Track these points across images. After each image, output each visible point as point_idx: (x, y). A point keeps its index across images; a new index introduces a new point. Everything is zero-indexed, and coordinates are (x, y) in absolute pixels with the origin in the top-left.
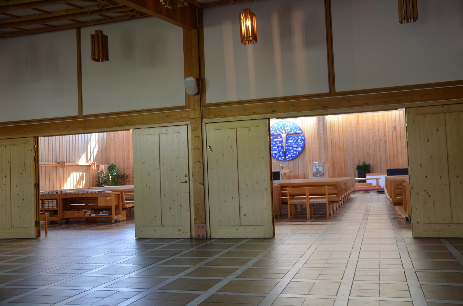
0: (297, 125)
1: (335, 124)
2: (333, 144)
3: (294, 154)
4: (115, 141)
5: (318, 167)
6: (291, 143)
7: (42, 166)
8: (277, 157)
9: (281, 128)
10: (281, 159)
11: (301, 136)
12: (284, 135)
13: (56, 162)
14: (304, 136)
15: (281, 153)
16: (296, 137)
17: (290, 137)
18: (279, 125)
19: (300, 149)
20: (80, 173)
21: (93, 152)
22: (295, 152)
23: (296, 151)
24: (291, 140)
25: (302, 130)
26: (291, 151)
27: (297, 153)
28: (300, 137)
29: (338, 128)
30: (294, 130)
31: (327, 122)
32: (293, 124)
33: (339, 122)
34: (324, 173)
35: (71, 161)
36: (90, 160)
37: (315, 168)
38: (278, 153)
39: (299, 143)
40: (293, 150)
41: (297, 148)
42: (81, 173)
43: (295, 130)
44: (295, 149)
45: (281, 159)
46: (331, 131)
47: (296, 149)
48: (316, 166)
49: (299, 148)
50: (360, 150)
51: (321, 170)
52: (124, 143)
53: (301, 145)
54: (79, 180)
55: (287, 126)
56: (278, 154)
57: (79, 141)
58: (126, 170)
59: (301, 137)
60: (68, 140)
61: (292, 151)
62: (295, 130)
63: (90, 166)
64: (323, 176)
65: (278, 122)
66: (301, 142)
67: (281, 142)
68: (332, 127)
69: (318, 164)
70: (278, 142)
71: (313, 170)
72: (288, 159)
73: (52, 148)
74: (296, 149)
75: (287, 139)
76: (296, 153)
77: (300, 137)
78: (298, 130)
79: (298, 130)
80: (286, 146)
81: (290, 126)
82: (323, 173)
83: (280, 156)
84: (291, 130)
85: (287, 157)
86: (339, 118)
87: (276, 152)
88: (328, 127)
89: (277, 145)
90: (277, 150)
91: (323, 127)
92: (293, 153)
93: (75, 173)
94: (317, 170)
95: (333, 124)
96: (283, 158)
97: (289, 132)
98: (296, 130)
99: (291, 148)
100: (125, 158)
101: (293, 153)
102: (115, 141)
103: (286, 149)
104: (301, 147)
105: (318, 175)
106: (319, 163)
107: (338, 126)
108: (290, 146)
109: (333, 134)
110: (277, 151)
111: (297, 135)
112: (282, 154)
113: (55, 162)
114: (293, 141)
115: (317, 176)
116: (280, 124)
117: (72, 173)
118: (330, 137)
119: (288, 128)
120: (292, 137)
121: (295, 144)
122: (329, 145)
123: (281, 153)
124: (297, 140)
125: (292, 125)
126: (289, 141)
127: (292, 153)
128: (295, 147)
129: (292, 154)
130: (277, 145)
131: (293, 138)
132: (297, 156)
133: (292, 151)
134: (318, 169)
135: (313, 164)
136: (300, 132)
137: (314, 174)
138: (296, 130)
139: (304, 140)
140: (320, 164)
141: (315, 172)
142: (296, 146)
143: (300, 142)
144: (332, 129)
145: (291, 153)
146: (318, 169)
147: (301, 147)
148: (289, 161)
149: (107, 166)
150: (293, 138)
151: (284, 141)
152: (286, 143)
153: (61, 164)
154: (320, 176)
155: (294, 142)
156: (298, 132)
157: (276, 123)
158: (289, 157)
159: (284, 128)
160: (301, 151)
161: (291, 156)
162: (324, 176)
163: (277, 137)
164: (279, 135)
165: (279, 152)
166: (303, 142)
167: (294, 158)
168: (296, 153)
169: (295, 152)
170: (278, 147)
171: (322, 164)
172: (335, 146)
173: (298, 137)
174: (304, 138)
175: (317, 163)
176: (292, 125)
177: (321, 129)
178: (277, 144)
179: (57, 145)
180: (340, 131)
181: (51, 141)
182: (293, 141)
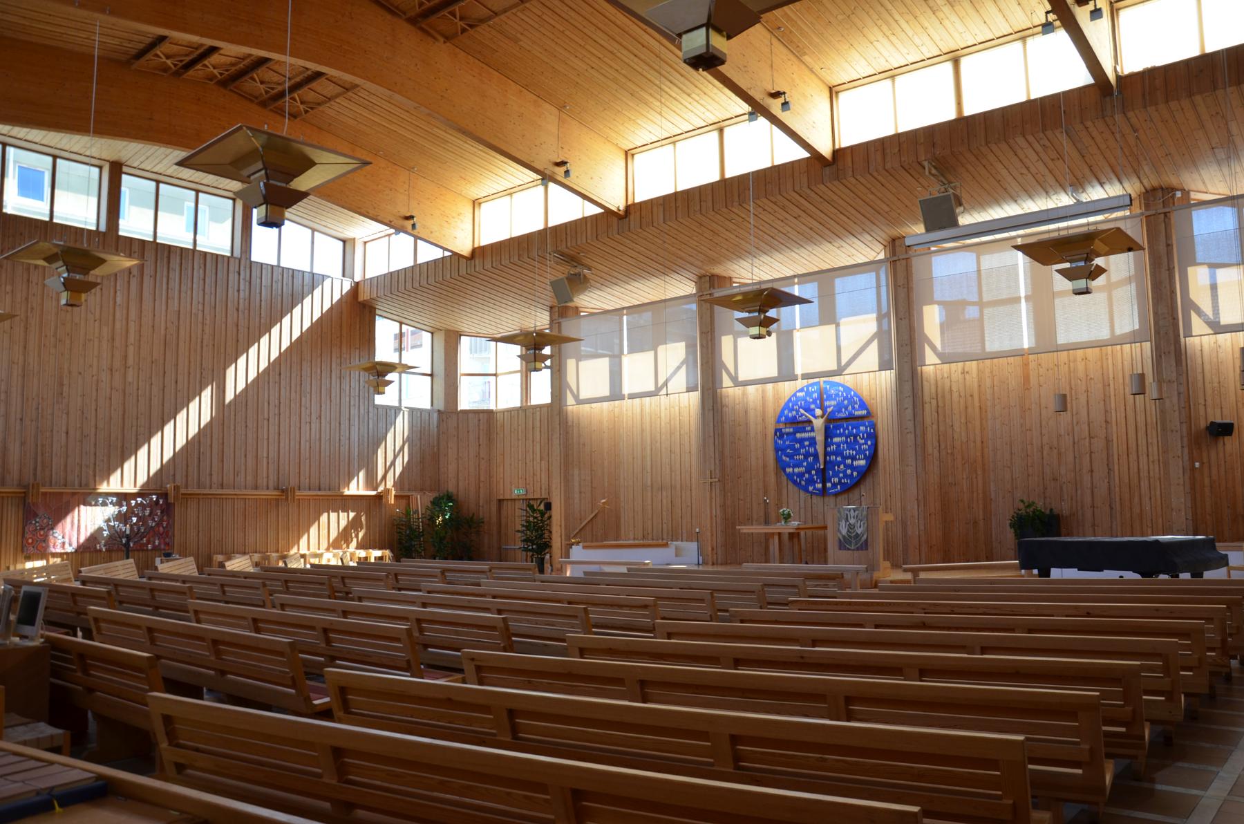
0: (856, 394)
1: (954, 389)
2: (946, 447)
3: (846, 476)
4: (458, 438)
5: (852, 521)
6: (838, 445)
7: (235, 497)
8: (803, 483)
9: (814, 402)
10: (815, 489)
11: (864, 425)
12: (819, 423)
13: (277, 488)
14: (874, 426)
15: (813, 472)
16: (852, 429)
17: (838, 428)
18: (809, 393)
19: (863, 462)
20: (341, 514)
21: (393, 463)
22: (849, 472)
23: (851, 467)
24: (840, 435)
25: (869, 407)
26: (839, 467)
27: (855, 474)
28: (862, 428)
29: (962, 401)
30: (846, 409)
31: (925, 383)
32: (844, 391)
33: (967, 383)
34: (869, 540)
35: (322, 486)
36: (383, 483)
37: (843, 523)
38: (806, 472)
39: (860, 445)
40: (846, 466)
41: (853, 458)
42: (352, 515)
43: (850, 408)
44: (849, 462)
45: (815, 489)
46: (940, 410)
47: (852, 462)
48: (847, 520)
49: (859, 459)
50: (766, 493)
51: (859, 531)
52: (479, 441)
53: (866, 450)
54: (345, 528)
55: (829, 397)
56: (807, 476)
57: (352, 440)
58: (483, 507)
59: (866, 427)
60: (318, 437)
61: (842, 466)
62: (850, 408)
63: (379, 497)
64: (867, 549)
65: (807, 386)
66: (866, 443)
67: (813, 442)
68: (943, 397)
69: (852, 511)
70: (807, 443)
71: (839, 531)
72: (830, 489)
73: (268, 457)
74: (852, 462)
75: (828, 434)
76: (852, 473)
77: (862, 428)
78: (856, 406)
79: (856, 406)
80: (826, 454)
81: (837, 395)
82: (866, 541)
83: (811, 481)
84: (839, 407)
85: (829, 485)
86: (966, 370)
87: (802, 470)
88: (927, 398)
89: (803, 451)
90: (805, 464)
91: (912, 398)
92: (845, 472)
93: (336, 514)
94: (848, 531)
95: (947, 389)
96: (819, 486)
97: (832, 412)
98: (853, 408)
99: (839, 459)
100: (482, 479)
101: (845, 472)
102: (458, 438)
103: (825, 462)
104: (865, 457)
105: (850, 545)
106: (854, 510)
107: (963, 394)
108: (837, 453)
109: (945, 417)
110: (803, 466)
111: (854, 422)
112: (816, 474)
113: (275, 489)
114: (844, 438)
115: (849, 549)
116: (813, 392)
117: (325, 515)
118: (935, 427)
119: (831, 404)
120: (843, 427)
121: (851, 448)
122: (930, 451)
123: (813, 472)
124: (855, 438)
125: (842, 394)
126: (836, 440)
127: (841, 472)
128: (848, 458)
129: (841, 475)
130: (803, 451)
131: (844, 430)
132: (855, 481)
133: (842, 466)
134: (851, 527)
135: (839, 512)
136: (864, 412)
137: (840, 540)
138: (853, 408)
139: (873, 437)
140: (857, 512)
141: (844, 537)
142: (853, 452)
143: (863, 441)
144: (940, 404)
145: (839, 472)
146: (851, 527)
147: (865, 455)
148: (836, 495)
149: (431, 496)
150: (844, 430)
151: (820, 438)
152: (826, 445)
153: (285, 493)
154: (858, 549)
155: (846, 442)
156: (857, 413)
157: (801, 390)
158: (834, 485)
159: (822, 401)
160: (865, 469)
161: (840, 482)
162: (869, 548)
163: (805, 428)
164: (810, 422)
165: (808, 472)
166: (869, 443)
167: (847, 489)
168: (852, 473)
169: (849, 472)
170: (807, 455)
171: (865, 513)
172: (952, 454)
173: (857, 428)
174: (874, 430)
175: (850, 510)
176: (842, 394)
177: (906, 406)
178: (805, 447)
179: (282, 451)
180: (970, 410)
181: (265, 442)
182: (844, 438)
